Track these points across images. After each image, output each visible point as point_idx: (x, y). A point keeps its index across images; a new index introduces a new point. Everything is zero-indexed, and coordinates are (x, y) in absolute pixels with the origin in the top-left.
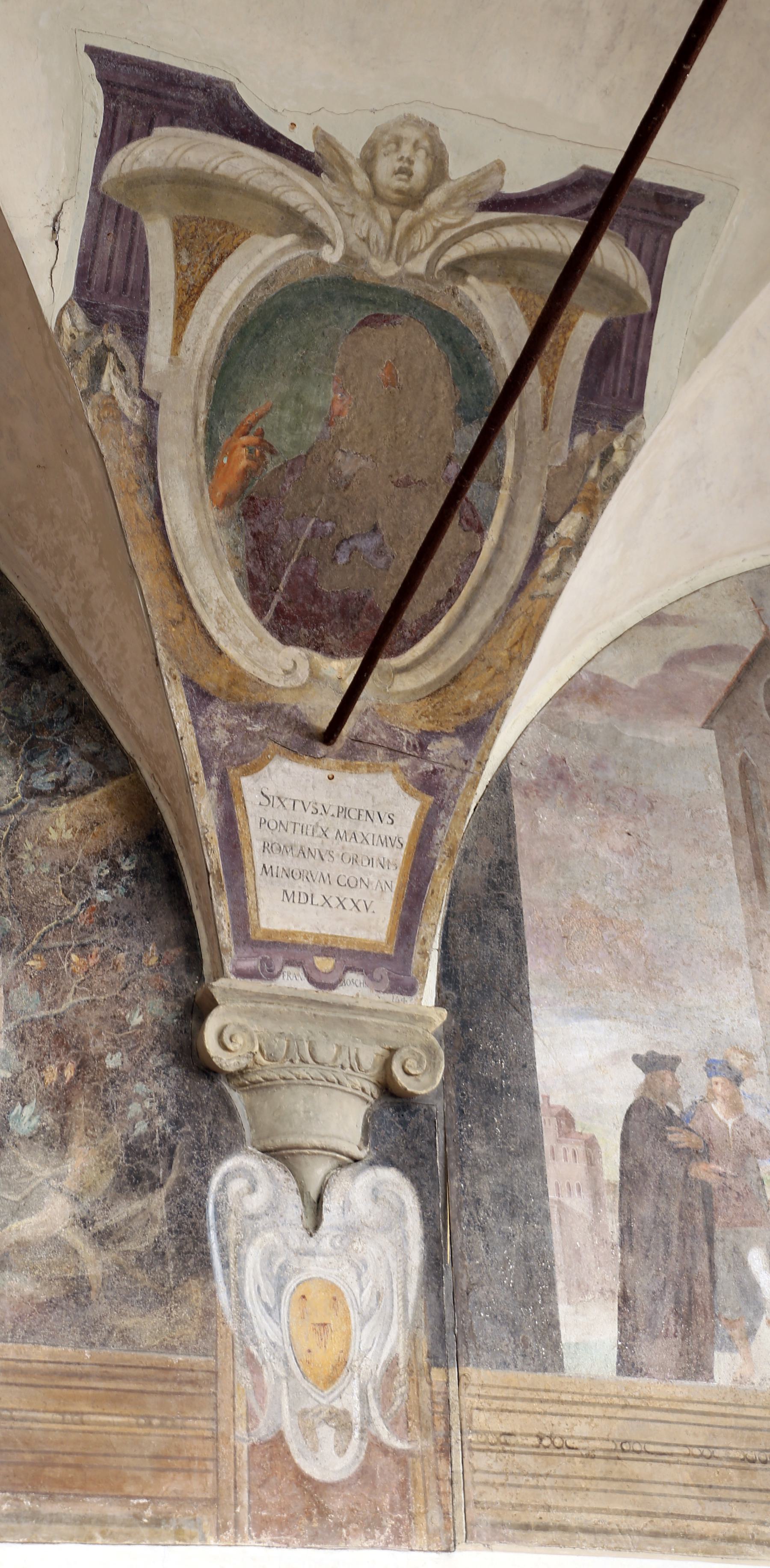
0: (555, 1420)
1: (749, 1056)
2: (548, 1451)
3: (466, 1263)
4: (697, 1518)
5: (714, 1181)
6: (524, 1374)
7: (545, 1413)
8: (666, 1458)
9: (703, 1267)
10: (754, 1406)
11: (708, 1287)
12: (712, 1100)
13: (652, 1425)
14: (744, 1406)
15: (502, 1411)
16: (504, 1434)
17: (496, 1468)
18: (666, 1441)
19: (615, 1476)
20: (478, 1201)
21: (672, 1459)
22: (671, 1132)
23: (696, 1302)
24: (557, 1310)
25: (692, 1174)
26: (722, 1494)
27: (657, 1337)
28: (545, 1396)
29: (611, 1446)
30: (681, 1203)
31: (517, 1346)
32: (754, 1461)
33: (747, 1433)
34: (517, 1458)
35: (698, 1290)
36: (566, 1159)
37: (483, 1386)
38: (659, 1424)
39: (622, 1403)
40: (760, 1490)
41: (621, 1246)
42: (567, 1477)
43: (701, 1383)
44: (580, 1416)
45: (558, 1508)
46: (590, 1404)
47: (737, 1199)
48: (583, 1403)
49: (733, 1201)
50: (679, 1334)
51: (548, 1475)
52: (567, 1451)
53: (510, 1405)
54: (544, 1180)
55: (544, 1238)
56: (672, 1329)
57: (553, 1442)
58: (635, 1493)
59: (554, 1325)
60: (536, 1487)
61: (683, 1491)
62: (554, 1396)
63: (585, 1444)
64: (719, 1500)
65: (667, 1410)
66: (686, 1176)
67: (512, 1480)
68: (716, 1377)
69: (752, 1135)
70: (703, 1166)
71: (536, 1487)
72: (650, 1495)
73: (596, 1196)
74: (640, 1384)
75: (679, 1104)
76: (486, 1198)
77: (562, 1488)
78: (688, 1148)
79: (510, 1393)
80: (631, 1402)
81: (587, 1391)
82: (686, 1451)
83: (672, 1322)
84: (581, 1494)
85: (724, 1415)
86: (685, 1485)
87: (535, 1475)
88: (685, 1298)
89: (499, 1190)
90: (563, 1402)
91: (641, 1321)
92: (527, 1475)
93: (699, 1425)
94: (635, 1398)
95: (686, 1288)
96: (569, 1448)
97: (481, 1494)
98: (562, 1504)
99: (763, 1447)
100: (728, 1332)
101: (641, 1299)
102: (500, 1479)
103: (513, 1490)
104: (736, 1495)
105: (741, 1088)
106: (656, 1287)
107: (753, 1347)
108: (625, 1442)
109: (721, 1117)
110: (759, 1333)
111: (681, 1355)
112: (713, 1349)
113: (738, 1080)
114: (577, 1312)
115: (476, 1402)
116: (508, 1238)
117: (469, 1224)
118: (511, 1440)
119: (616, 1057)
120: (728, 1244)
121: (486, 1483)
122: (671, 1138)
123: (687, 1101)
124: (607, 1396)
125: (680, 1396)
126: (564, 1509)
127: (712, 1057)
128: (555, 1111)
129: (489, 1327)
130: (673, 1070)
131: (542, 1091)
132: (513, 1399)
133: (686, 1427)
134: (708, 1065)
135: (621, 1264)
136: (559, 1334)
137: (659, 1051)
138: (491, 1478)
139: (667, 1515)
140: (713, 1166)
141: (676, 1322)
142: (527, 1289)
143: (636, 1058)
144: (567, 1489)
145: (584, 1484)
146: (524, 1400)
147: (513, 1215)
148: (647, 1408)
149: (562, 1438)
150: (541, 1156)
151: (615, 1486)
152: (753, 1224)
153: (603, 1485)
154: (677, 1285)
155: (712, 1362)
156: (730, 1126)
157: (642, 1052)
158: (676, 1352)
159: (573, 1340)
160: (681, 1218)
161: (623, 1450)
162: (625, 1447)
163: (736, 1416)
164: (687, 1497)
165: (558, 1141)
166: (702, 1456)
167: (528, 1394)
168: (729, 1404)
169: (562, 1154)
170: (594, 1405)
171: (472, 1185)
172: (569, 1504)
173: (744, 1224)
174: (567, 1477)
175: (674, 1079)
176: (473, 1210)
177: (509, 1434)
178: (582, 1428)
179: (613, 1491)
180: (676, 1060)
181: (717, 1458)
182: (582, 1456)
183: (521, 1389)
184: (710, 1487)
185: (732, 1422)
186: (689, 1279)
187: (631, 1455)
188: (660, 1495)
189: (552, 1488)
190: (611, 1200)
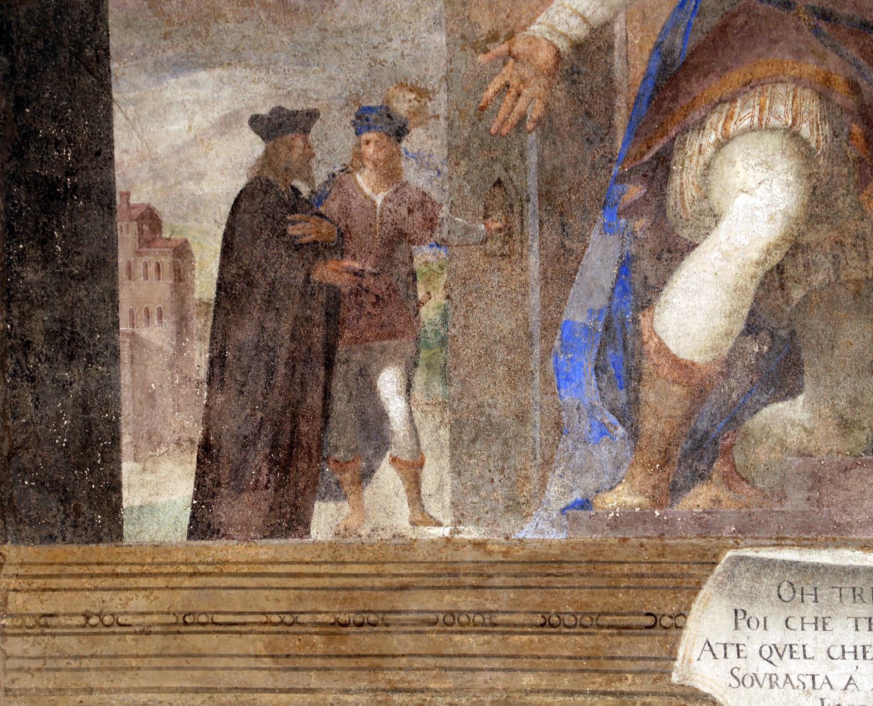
0: (106, 596)
1: (422, 93)
2: (95, 630)
3: (9, 423)
4: (266, 690)
5: (344, 283)
6: (75, 548)
7: (96, 589)
8: (237, 628)
9: (314, 399)
10: (357, 563)
11: (318, 424)
12: (357, 169)
13: (224, 593)
14: (343, 563)
15: (44, 590)
16: (45, 615)
17: (32, 652)
18: (238, 609)
19: (173, 651)
20: (27, 345)
21: (244, 629)
22: (294, 223)
23: (299, 443)
24: (120, 469)
25: (315, 277)
26: (301, 663)
27: (242, 491)
28: (97, 570)
29: (173, 619)
30: (296, 318)
31: (68, 516)
32: (346, 625)
33: (343, 594)
34: (58, 640)
35: (304, 428)
36: (146, 277)
37: (22, 564)
38: (233, 592)
39: (191, 570)
40: (349, 656)
41: (209, 384)
42: (116, 656)
43: (293, 541)
44: (138, 589)
45: (101, 690)
46: (151, 575)
47: (374, 305)
48: (142, 575)
49: (369, 308)
50: (272, 485)
51: (93, 656)
52: (117, 629)
53: (54, 583)
54: (116, 307)
55: (111, 384)
56: (264, 479)
57: (102, 620)
58: (194, 669)
59: (116, 487)
60: (79, 669)
61: (253, 663)
62: (108, 569)
63: (140, 620)
64: (296, 669)
65: (245, 575)
66: (307, 281)
67: (50, 664)
68: (313, 532)
69: (410, 211)
70: (332, 265)
71: (79, 669)
72: (213, 669)
73: (182, 322)
74: (216, 548)
75: (309, 180)
76: (38, 339)
77: (108, 669)
78: (316, 242)
79: (55, 570)
80: (202, 568)
81: (149, 560)
82: (263, 619)
83: (265, 471)
84: (131, 673)
85: (317, 575)
86: (257, 656)
87: (77, 657)
88: (285, 440)
89: (56, 327)
90: (118, 575)
91: (225, 472)
92: (69, 657)
93: (284, 588)
94: (208, 564)
95: (288, 427)
96: (121, 625)
97: (13, 681)
98: (106, 685)
99: (361, 607)
100: (337, 476)
101: (229, 449)
102: (39, 664)
103: (51, 675)
104: (318, 662)
105: (404, 144)
106: (248, 430)
107: (367, 492)
108: (189, 614)
109: (368, 191)
110: (378, 474)
111: (271, 510)
112: (314, 499)
113: (400, 133)
114: (144, 470)
115: (13, 583)
116: (64, 387)
117: (14, 376)
118: (53, 621)
119: (226, 124)
120: (352, 365)
121: (20, 669)
122: (292, 231)
123: (321, 175)
124: (172, 564)
125: (264, 557)
126: (109, 691)
127: (365, 104)
128: (136, 213)
129: (34, 497)
130: (306, 131)
131: (120, 186)
132: (58, 576)
133: (267, 592)
134: (358, 117)
135: (207, 406)
136: (120, 498)
137: (289, 105)
138: (27, 664)
139: (229, 690)
140: (347, 263)
141: (270, 470)
142: (84, 448)
143: (255, 122)
144: (114, 669)
145: (134, 663)
146: (71, 576)
147: (71, 357)
148: (221, 574)
149: (112, 615)
150: (113, 277)
151: (171, 662)
152: (392, 336)
153: (156, 662)
154: (278, 426)
155: (311, 514)
156: (379, 202)
157: (264, 111)
158: (265, 506)
159: (137, 503)
160: (293, 338)
161: (186, 623)
162: (188, 619)
163: (332, 576)
164: (258, 669)
165: (138, 253)
166: (282, 623)
167: (76, 570)
168: (326, 563)
169: (140, 271)
170: (155, 575)
171: (21, 325)
172: (115, 685)
173: (379, 337)
174: (116, 656)
175: (307, 145)
176: (20, 355)
177: (51, 615)
178: (139, 602)
179: (168, 668)
180: (312, 115)
181: (300, 624)
182: (135, 633)
183: (69, 564)
184: (288, 656)
185: (326, 582)
186: (294, 416)
187: (194, 628)
188: (225, 669)
189: (97, 669)
190: (201, 325)
